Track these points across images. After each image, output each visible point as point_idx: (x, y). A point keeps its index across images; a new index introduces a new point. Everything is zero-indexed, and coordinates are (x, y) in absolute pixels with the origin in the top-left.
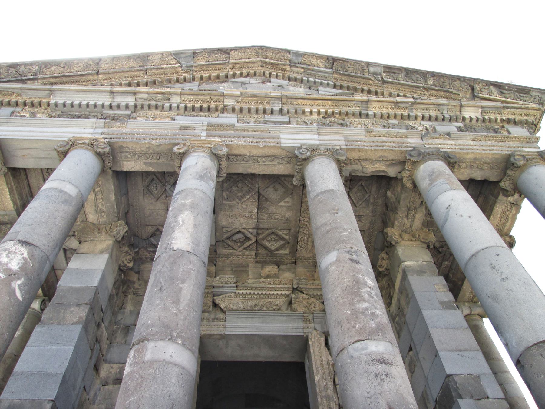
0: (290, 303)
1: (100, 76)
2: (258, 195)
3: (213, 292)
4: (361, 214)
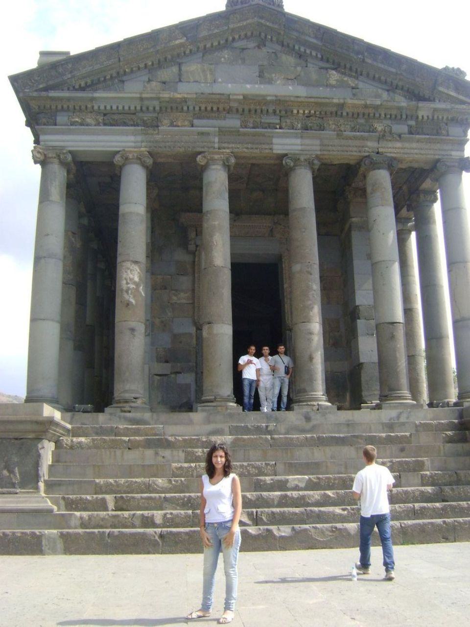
0: (271, 231)
1: (121, 63)
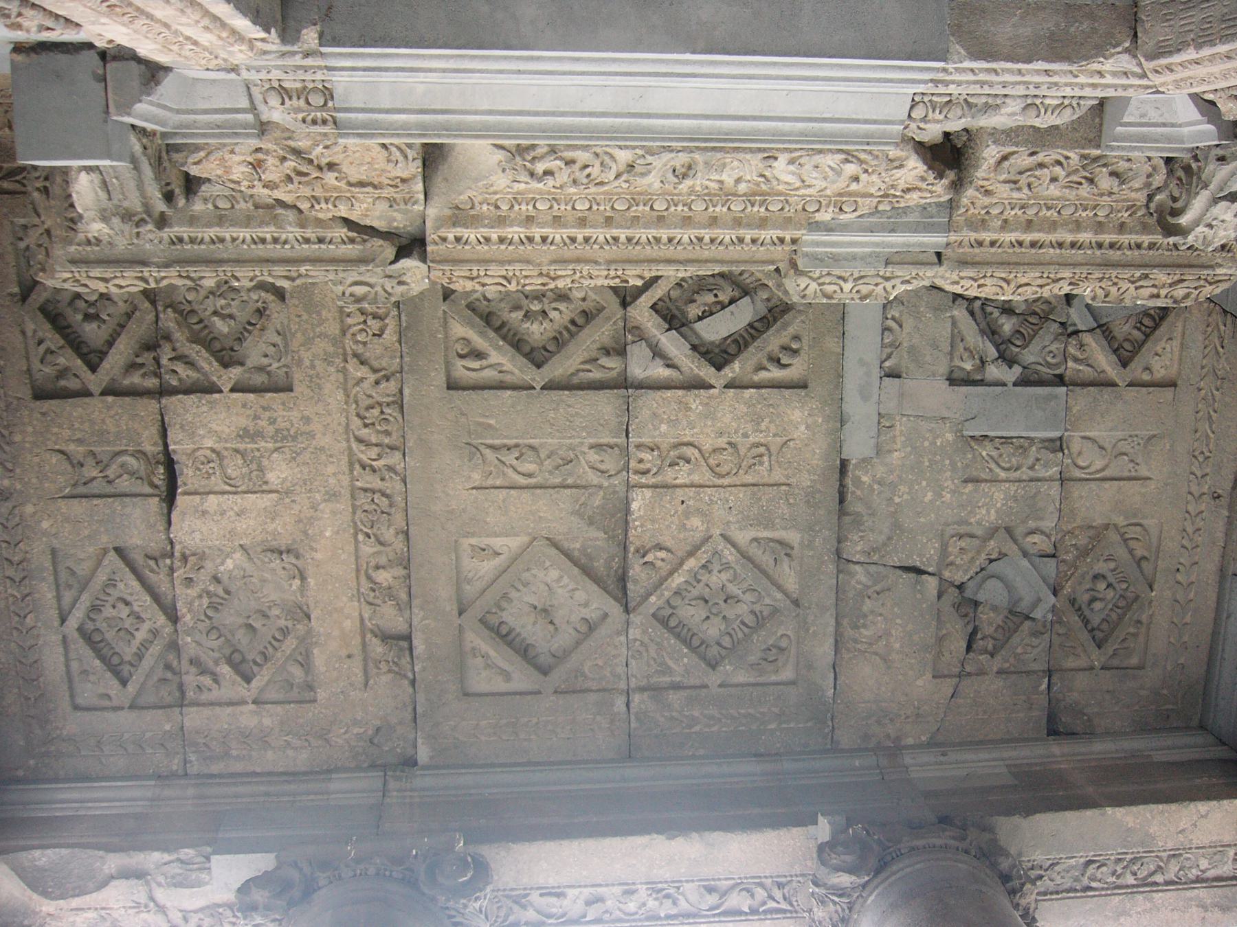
2: (630, 586)
3: (949, 227)
4: (78, 508)
